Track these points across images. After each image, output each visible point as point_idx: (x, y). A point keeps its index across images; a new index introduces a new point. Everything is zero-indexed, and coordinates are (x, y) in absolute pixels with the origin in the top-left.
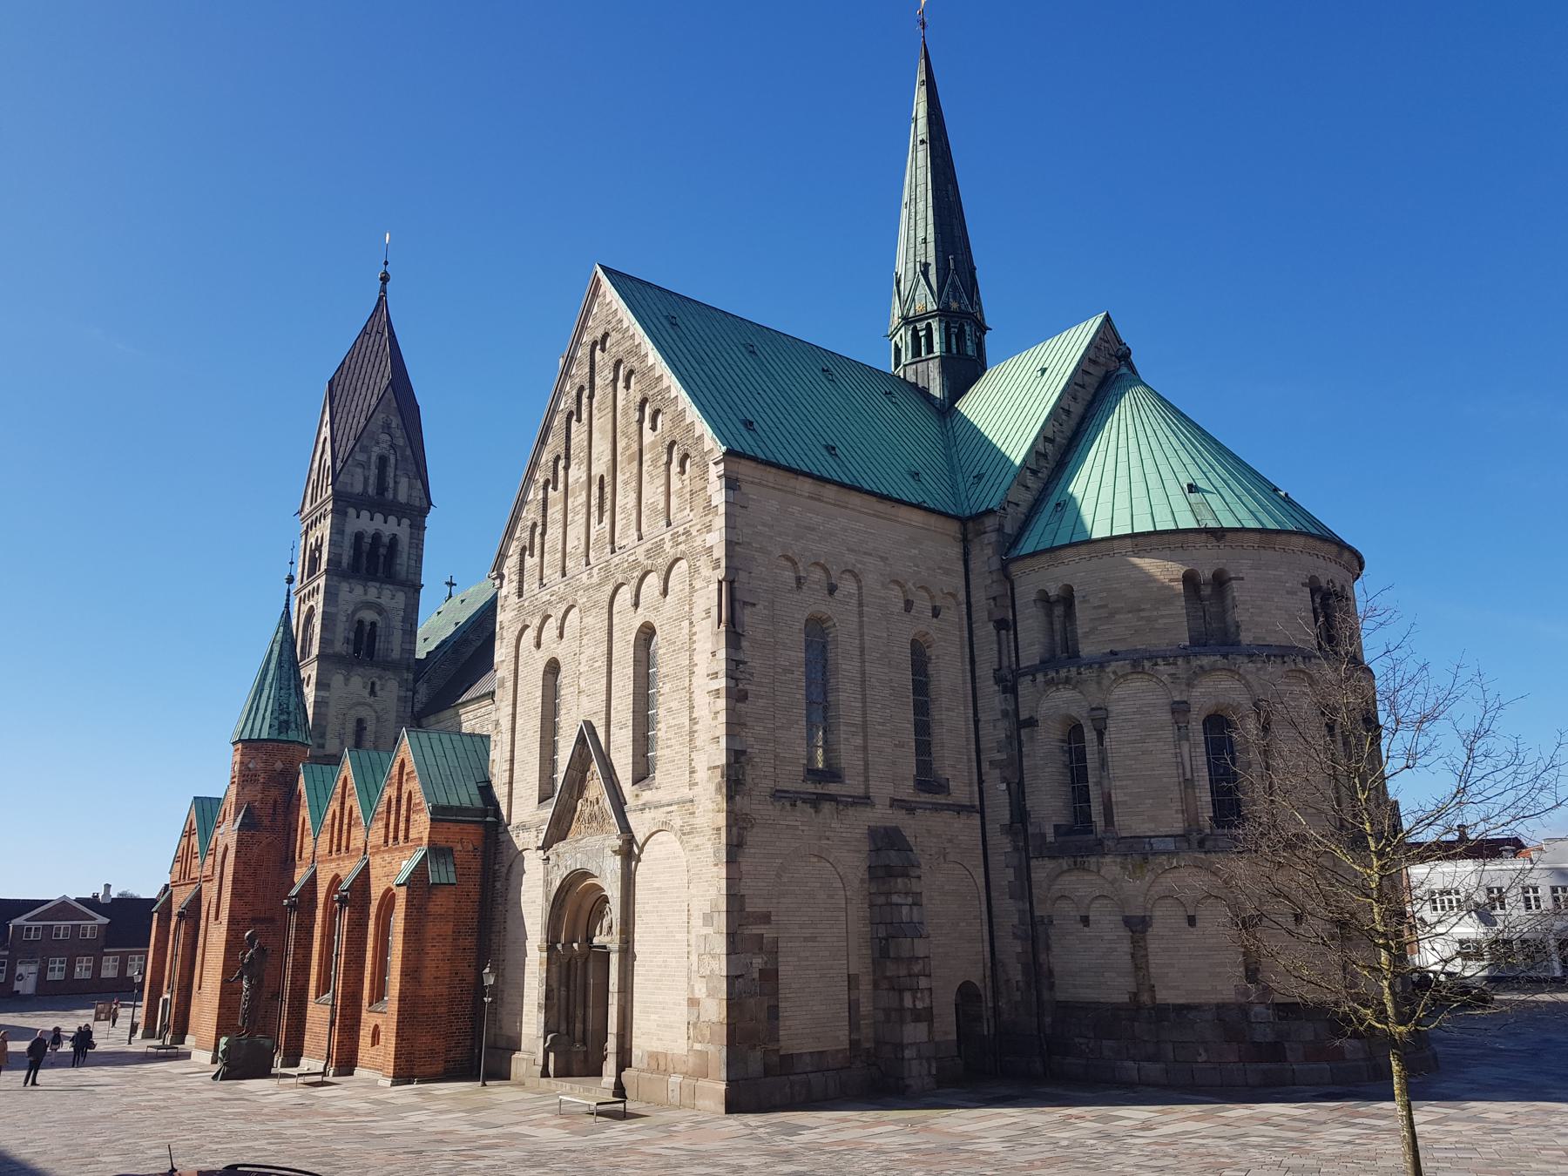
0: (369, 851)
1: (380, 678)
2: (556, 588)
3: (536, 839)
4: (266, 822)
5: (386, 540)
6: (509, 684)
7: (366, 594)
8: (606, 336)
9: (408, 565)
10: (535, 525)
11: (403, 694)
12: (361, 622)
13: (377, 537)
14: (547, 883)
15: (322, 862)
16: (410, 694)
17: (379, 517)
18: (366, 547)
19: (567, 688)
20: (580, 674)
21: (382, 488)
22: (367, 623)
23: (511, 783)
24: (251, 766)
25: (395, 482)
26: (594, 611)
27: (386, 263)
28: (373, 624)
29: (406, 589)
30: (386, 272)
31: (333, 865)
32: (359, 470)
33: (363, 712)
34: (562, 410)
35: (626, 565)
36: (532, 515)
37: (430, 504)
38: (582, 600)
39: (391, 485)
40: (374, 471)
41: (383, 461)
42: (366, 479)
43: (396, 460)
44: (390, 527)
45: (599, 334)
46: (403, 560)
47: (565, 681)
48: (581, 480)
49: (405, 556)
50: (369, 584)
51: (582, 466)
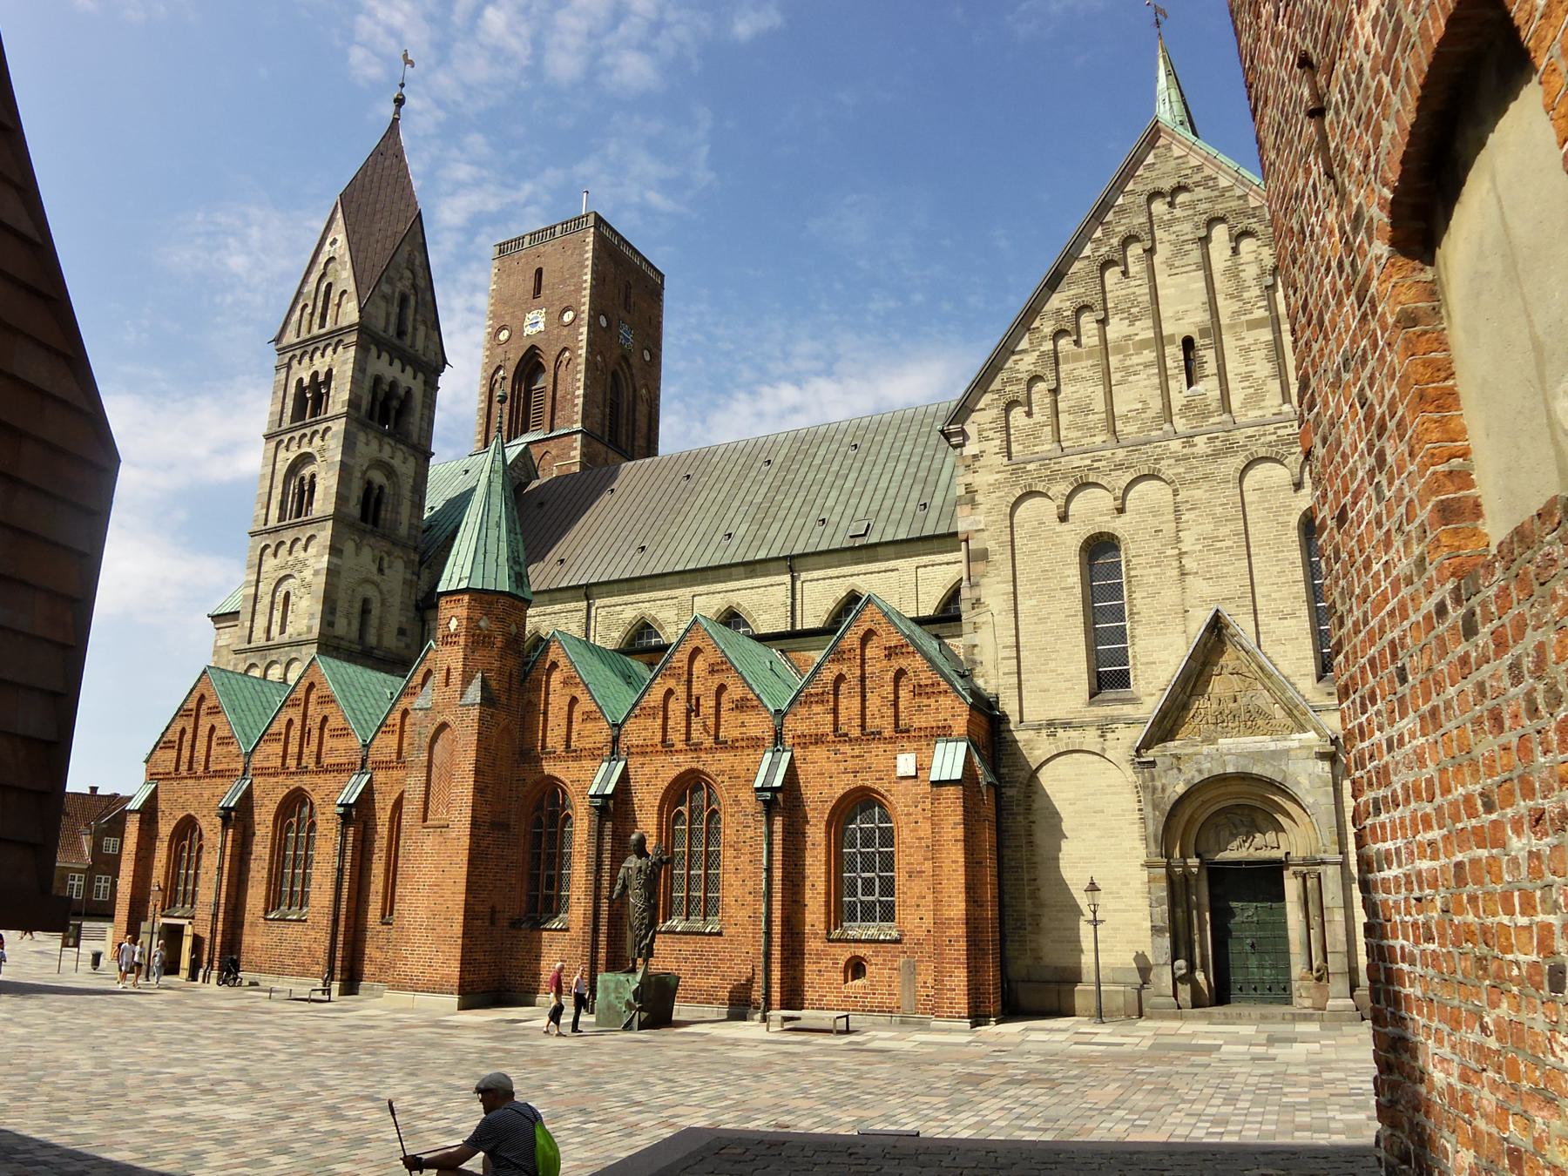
0: (788, 740)
1: (389, 554)
2: (1108, 453)
4: (504, 700)
5: (402, 392)
6: (1000, 557)
7: (380, 451)
8: (1180, 188)
9: (421, 429)
10: (1035, 379)
11: (408, 576)
12: (369, 483)
13: (394, 384)
14: (1148, 789)
15: (644, 754)
16: (415, 578)
17: (397, 364)
18: (381, 397)
19: (1145, 568)
20: (1181, 554)
21: (401, 333)
22: (376, 486)
23: (1019, 673)
24: (482, 624)
25: (415, 329)
26: (1206, 486)
27: (402, 85)
28: (381, 488)
29: (418, 454)
30: (401, 94)
31: (681, 758)
32: (383, 304)
33: (370, 592)
34: (1088, 257)
35: (1274, 437)
36: (1031, 367)
37: (445, 362)
38: (1168, 469)
39: (410, 329)
40: (395, 309)
41: (404, 300)
42: (388, 315)
43: (417, 302)
44: (407, 379)
45: (1167, 185)
46: (415, 420)
47: (1134, 561)
48: (1137, 338)
49: (417, 415)
50: (387, 440)
51: (1137, 323)
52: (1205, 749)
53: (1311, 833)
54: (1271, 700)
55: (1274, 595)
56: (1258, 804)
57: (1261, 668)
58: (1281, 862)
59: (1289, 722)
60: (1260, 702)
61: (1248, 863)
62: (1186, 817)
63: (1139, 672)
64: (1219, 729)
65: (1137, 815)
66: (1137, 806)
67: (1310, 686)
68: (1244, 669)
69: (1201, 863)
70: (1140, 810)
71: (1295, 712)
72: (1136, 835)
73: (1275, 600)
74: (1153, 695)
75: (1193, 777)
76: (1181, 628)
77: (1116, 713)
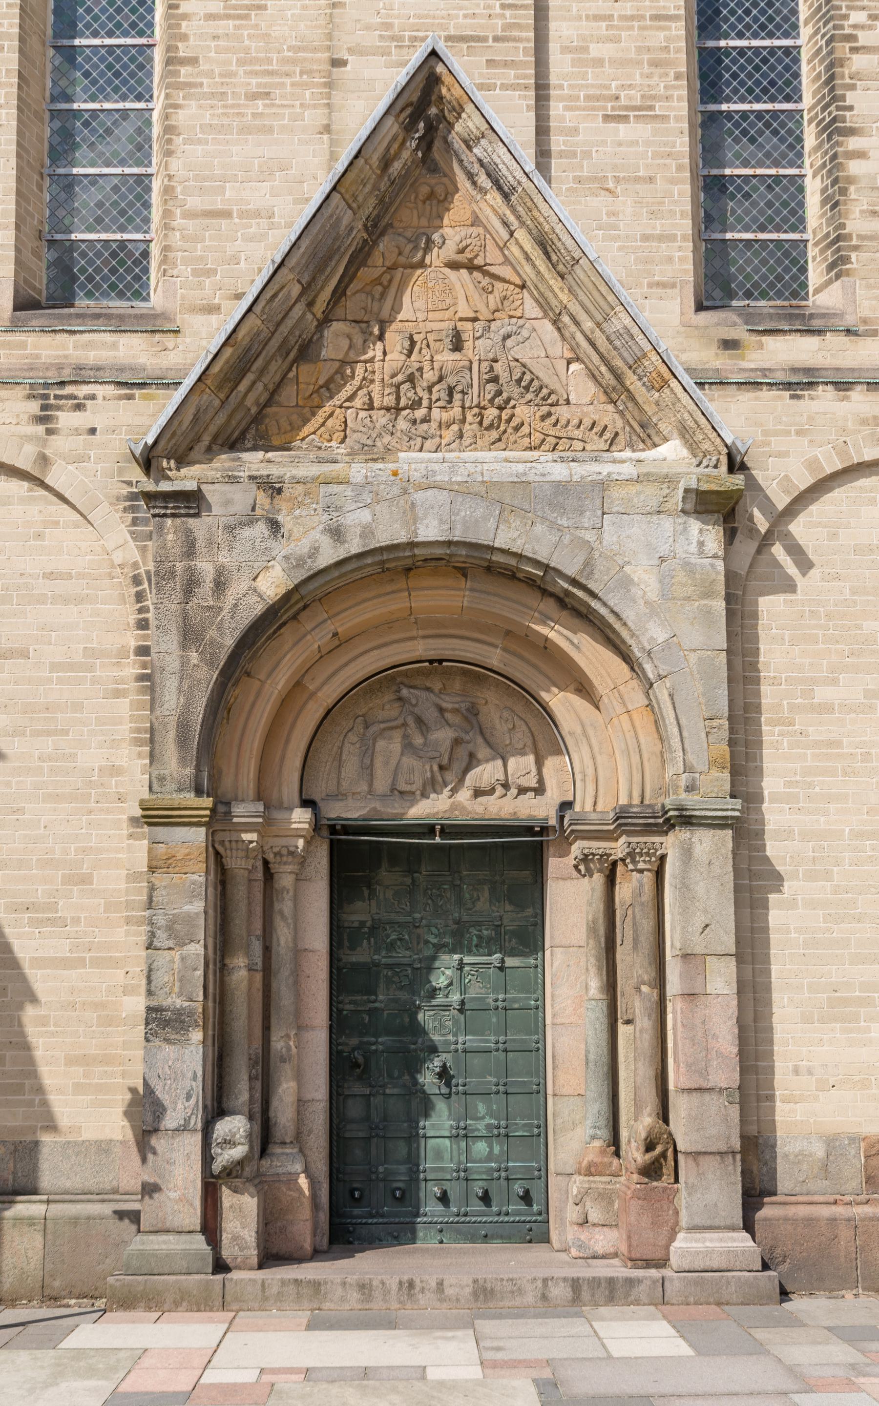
3: (41, 429)
52: (358, 471)
53: (648, 740)
54: (559, 349)
55: (596, 50)
56: (495, 658)
57: (544, 244)
58: (544, 830)
59: (608, 416)
60: (527, 353)
61: (447, 831)
62: (281, 681)
63: (176, 238)
64: (402, 424)
65: (131, 668)
66: (131, 639)
67: (676, 320)
68: (492, 255)
69: (317, 827)
70: (143, 651)
71: (631, 380)
72: (125, 730)
73: (599, 62)
74: (212, 309)
75: (314, 552)
76: (315, 117)
77: (92, 357)
